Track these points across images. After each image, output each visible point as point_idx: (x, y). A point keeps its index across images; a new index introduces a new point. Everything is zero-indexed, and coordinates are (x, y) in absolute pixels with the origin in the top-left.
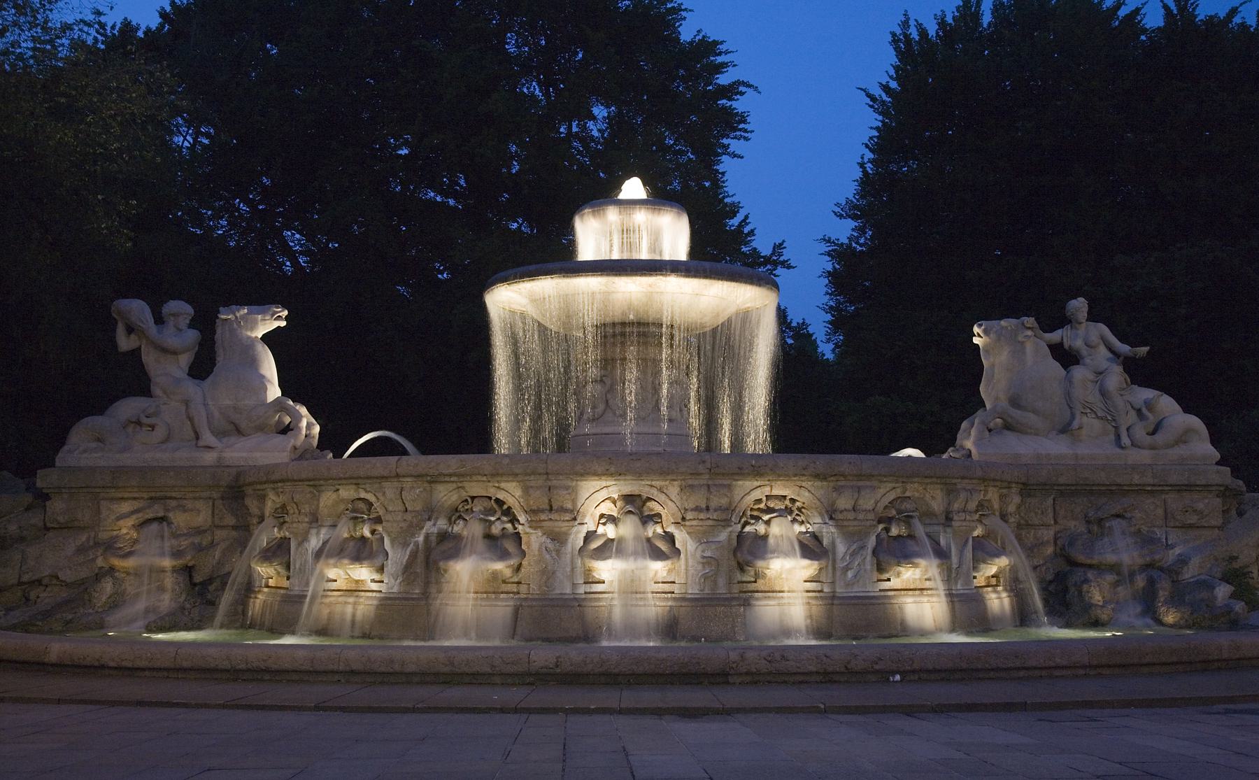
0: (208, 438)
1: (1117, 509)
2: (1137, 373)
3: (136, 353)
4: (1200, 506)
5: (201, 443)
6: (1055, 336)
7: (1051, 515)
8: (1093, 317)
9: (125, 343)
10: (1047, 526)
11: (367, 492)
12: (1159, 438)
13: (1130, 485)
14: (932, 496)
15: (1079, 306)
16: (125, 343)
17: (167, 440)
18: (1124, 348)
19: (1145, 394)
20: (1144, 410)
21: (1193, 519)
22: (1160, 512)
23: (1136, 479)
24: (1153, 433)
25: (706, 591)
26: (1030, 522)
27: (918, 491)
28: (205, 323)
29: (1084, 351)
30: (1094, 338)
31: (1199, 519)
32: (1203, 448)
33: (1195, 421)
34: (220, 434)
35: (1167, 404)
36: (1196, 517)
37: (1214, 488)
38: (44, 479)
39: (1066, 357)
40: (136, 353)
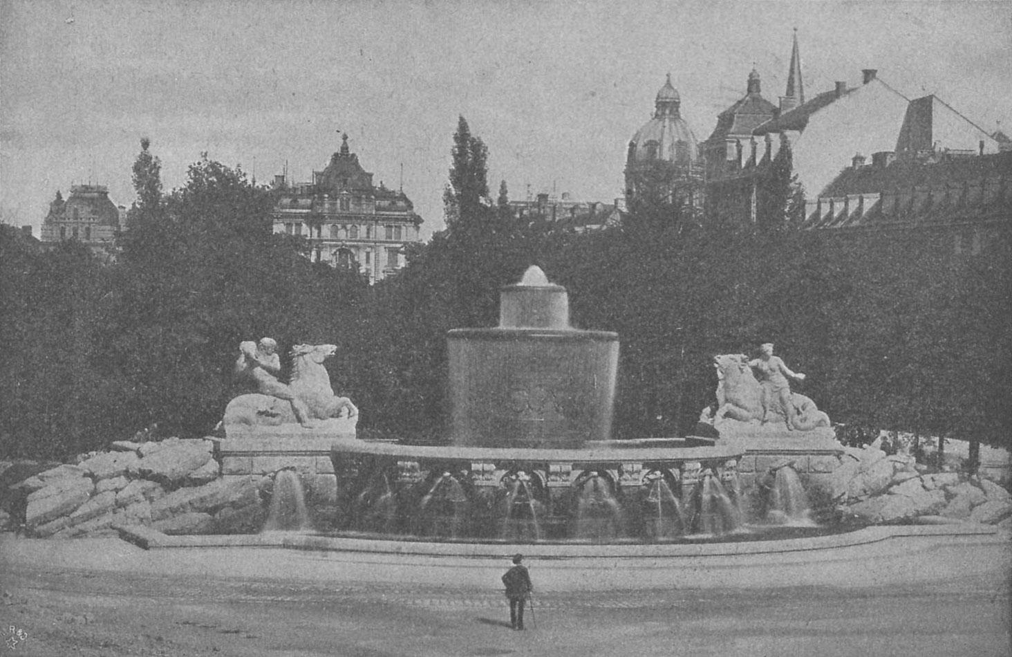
2: (795, 386)
15: (768, 347)
30: (774, 366)
39: (759, 374)
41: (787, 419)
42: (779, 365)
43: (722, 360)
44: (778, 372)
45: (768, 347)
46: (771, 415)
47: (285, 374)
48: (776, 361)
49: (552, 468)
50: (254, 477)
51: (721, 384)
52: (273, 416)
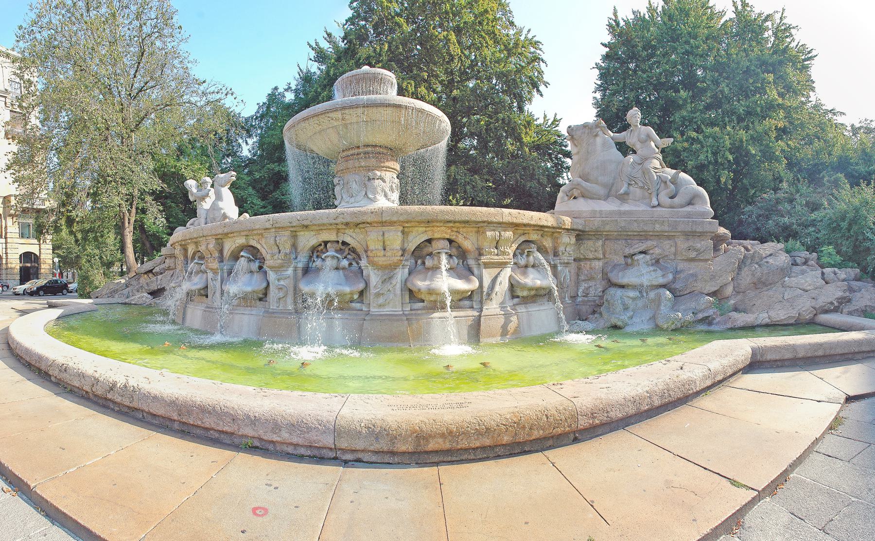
1: (643, 247)
4: (699, 245)
7: (601, 252)
13: (653, 231)
14: (464, 237)
21: (693, 255)
22: (673, 249)
23: (658, 227)
24: (672, 198)
25: (281, 308)
26: (587, 257)
27: (446, 233)
31: (697, 255)
36: (695, 253)
37: (709, 234)
39: (624, 148)
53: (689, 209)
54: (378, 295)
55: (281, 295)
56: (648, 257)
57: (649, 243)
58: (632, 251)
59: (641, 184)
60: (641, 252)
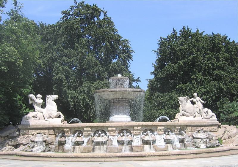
0: (46, 119)
2: (205, 106)
3: (32, 104)
5: (45, 120)
6: (192, 99)
8: (198, 96)
9: (30, 102)
10: (190, 132)
11: (80, 129)
12: (208, 117)
15: (195, 94)
16: (30, 102)
17: (39, 120)
18: (203, 102)
19: (206, 109)
20: (206, 112)
21: (213, 130)
28: (44, 98)
29: (196, 102)
30: (198, 100)
32: (215, 118)
33: (214, 114)
34: (48, 118)
35: (210, 111)
38: (20, 127)
39: (193, 103)
40: (32, 104)
41: (201, 115)
42: (199, 100)
43: (181, 98)
44: (199, 101)
45: (195, 94)
46: (197, 114)
47: (44, 106)
48: (198, 98)
49: (109, 129)
50: (29, 136)
51: (181, 106)
52: (37, 117)
53: (211, 119)
54: (159, 140)
55: (138, 141)
56: (202, 131)
57: (202, 128)
58: (199, 130)
59: (199, 113)
60: (201, 130)
